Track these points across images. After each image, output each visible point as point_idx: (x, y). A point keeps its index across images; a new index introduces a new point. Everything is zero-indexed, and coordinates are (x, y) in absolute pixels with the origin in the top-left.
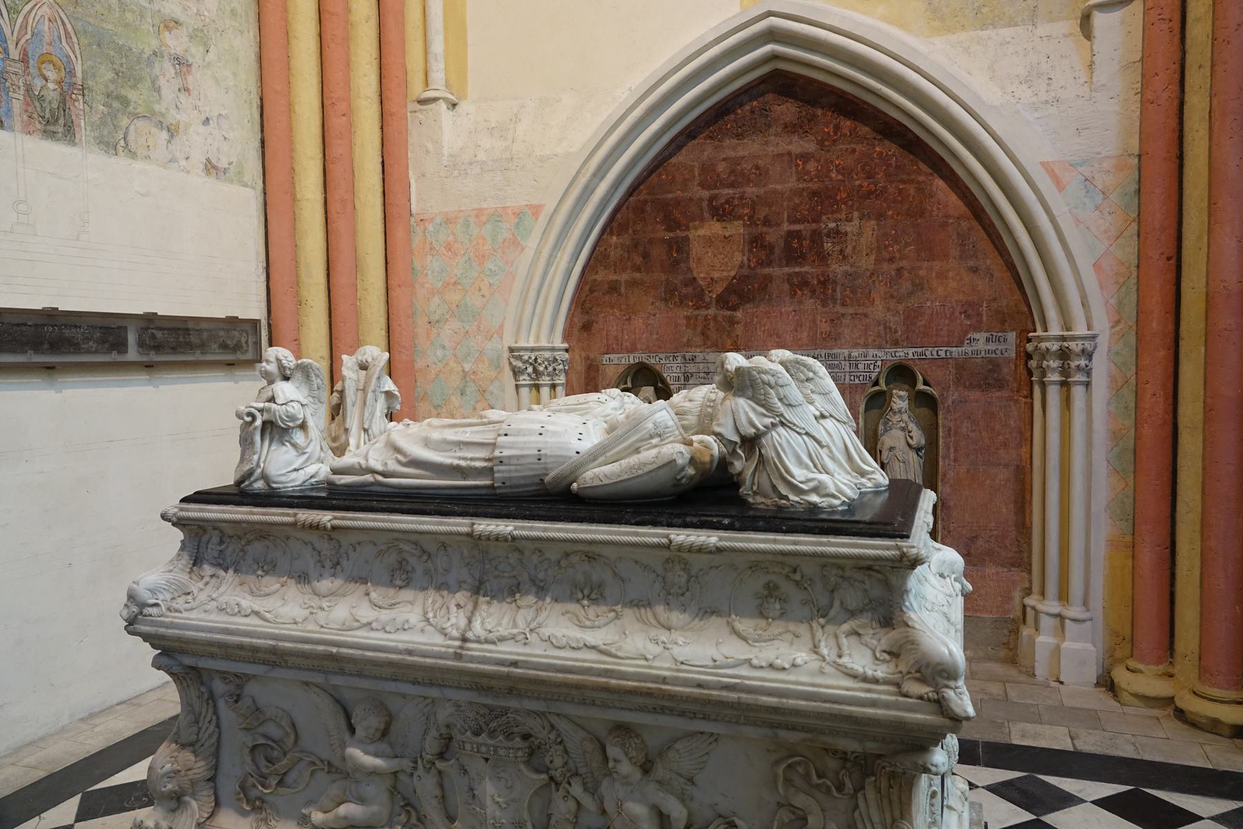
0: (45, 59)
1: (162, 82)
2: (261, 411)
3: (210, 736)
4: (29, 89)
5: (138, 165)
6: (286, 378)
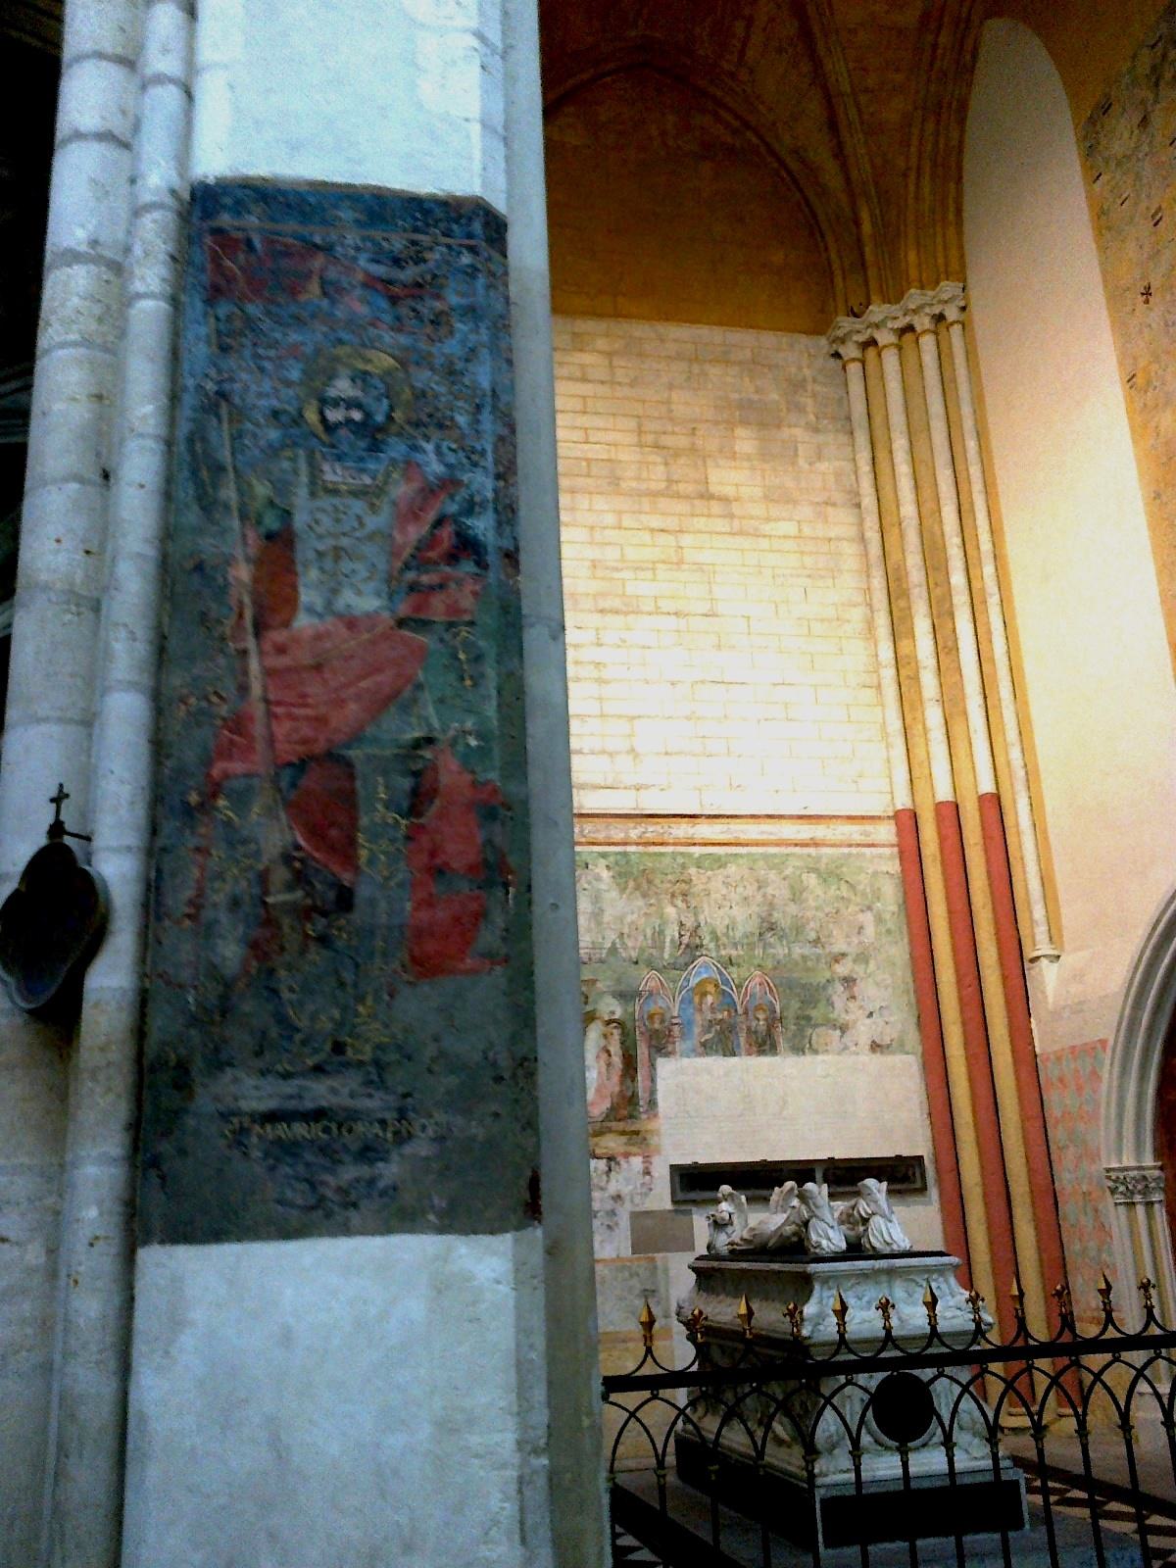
0: (758, 1008)
1: (835, 998)
4: (749, 1029)
5: (820, 1057)
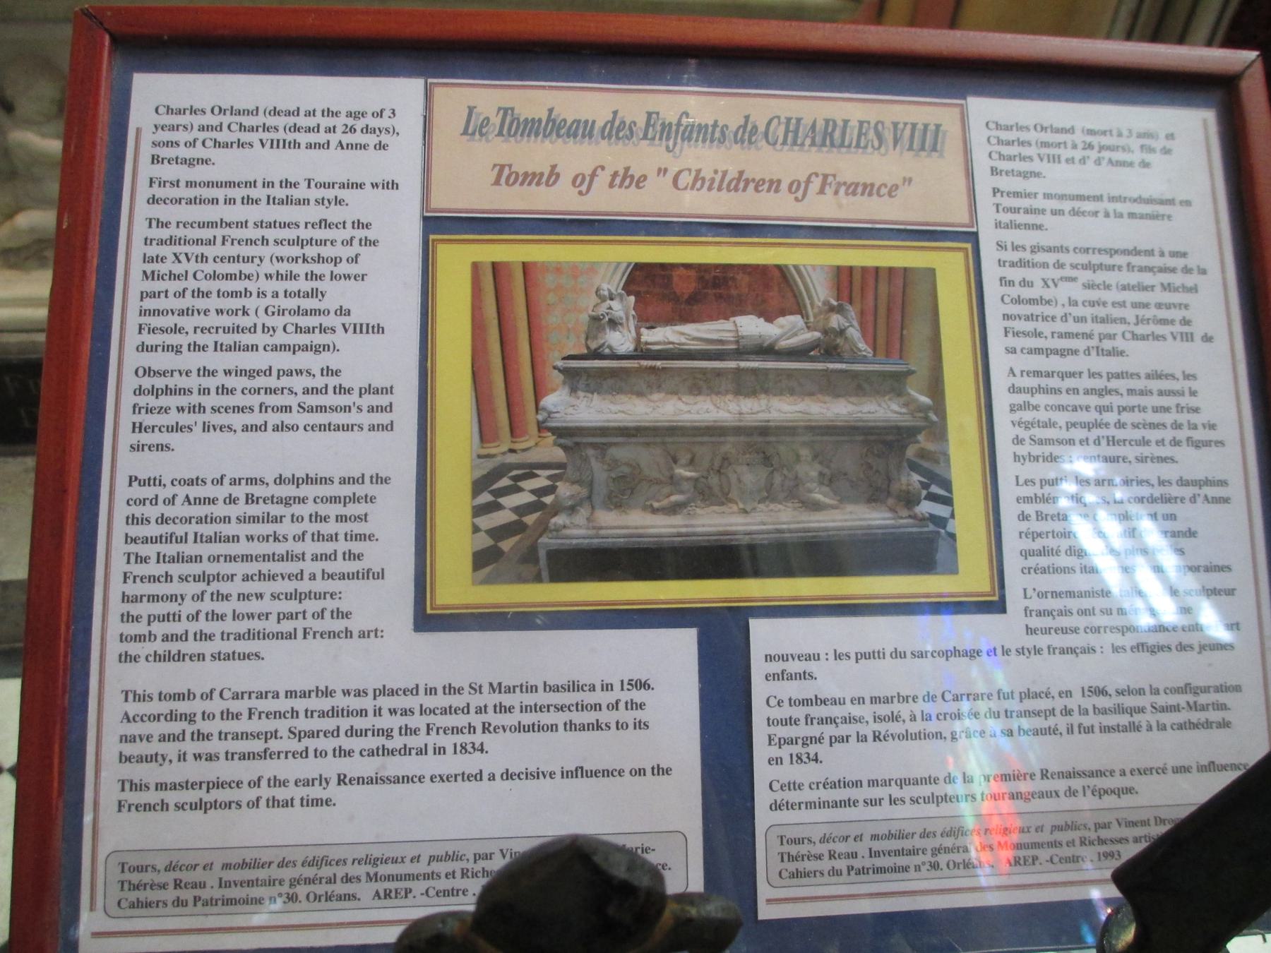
6: (612, 299)
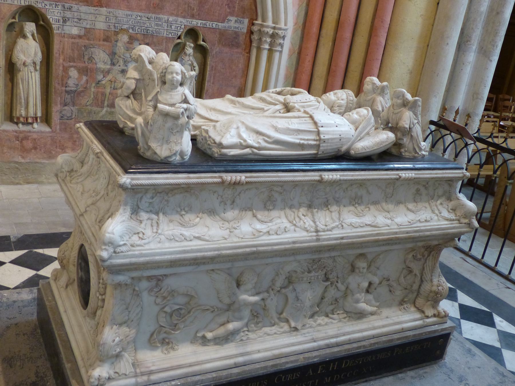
2: (186, 110)
3: (137, 314)
